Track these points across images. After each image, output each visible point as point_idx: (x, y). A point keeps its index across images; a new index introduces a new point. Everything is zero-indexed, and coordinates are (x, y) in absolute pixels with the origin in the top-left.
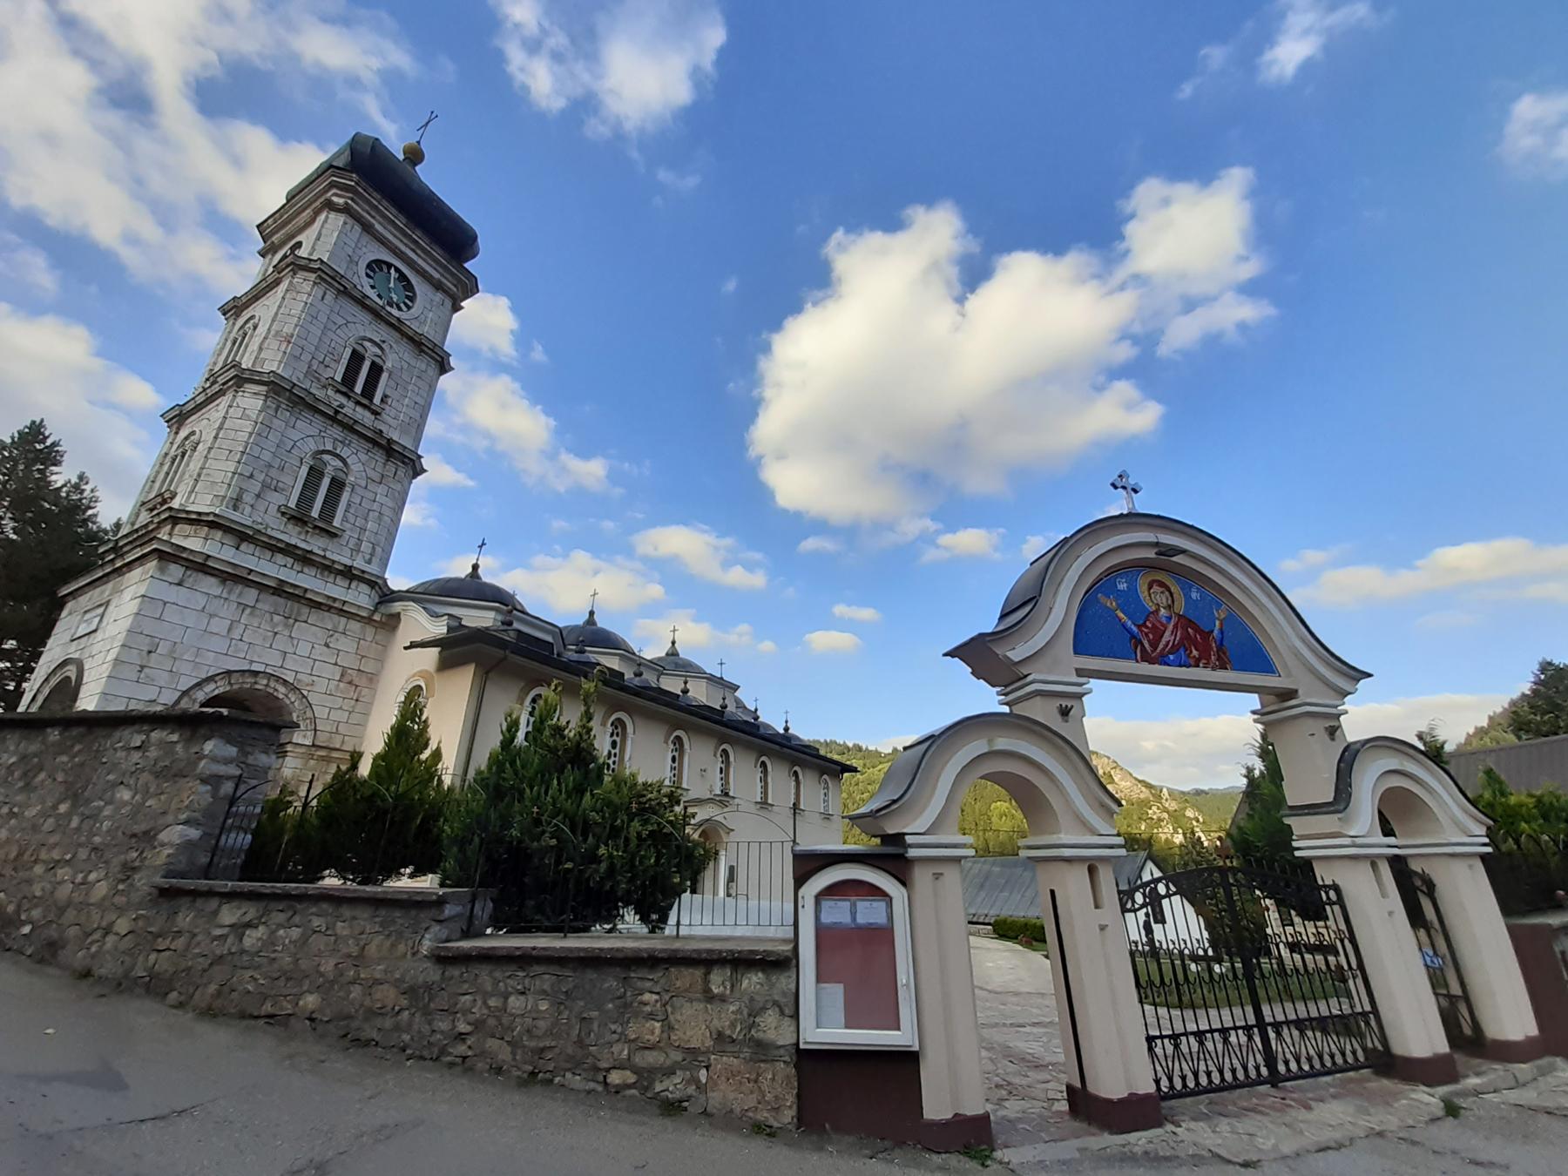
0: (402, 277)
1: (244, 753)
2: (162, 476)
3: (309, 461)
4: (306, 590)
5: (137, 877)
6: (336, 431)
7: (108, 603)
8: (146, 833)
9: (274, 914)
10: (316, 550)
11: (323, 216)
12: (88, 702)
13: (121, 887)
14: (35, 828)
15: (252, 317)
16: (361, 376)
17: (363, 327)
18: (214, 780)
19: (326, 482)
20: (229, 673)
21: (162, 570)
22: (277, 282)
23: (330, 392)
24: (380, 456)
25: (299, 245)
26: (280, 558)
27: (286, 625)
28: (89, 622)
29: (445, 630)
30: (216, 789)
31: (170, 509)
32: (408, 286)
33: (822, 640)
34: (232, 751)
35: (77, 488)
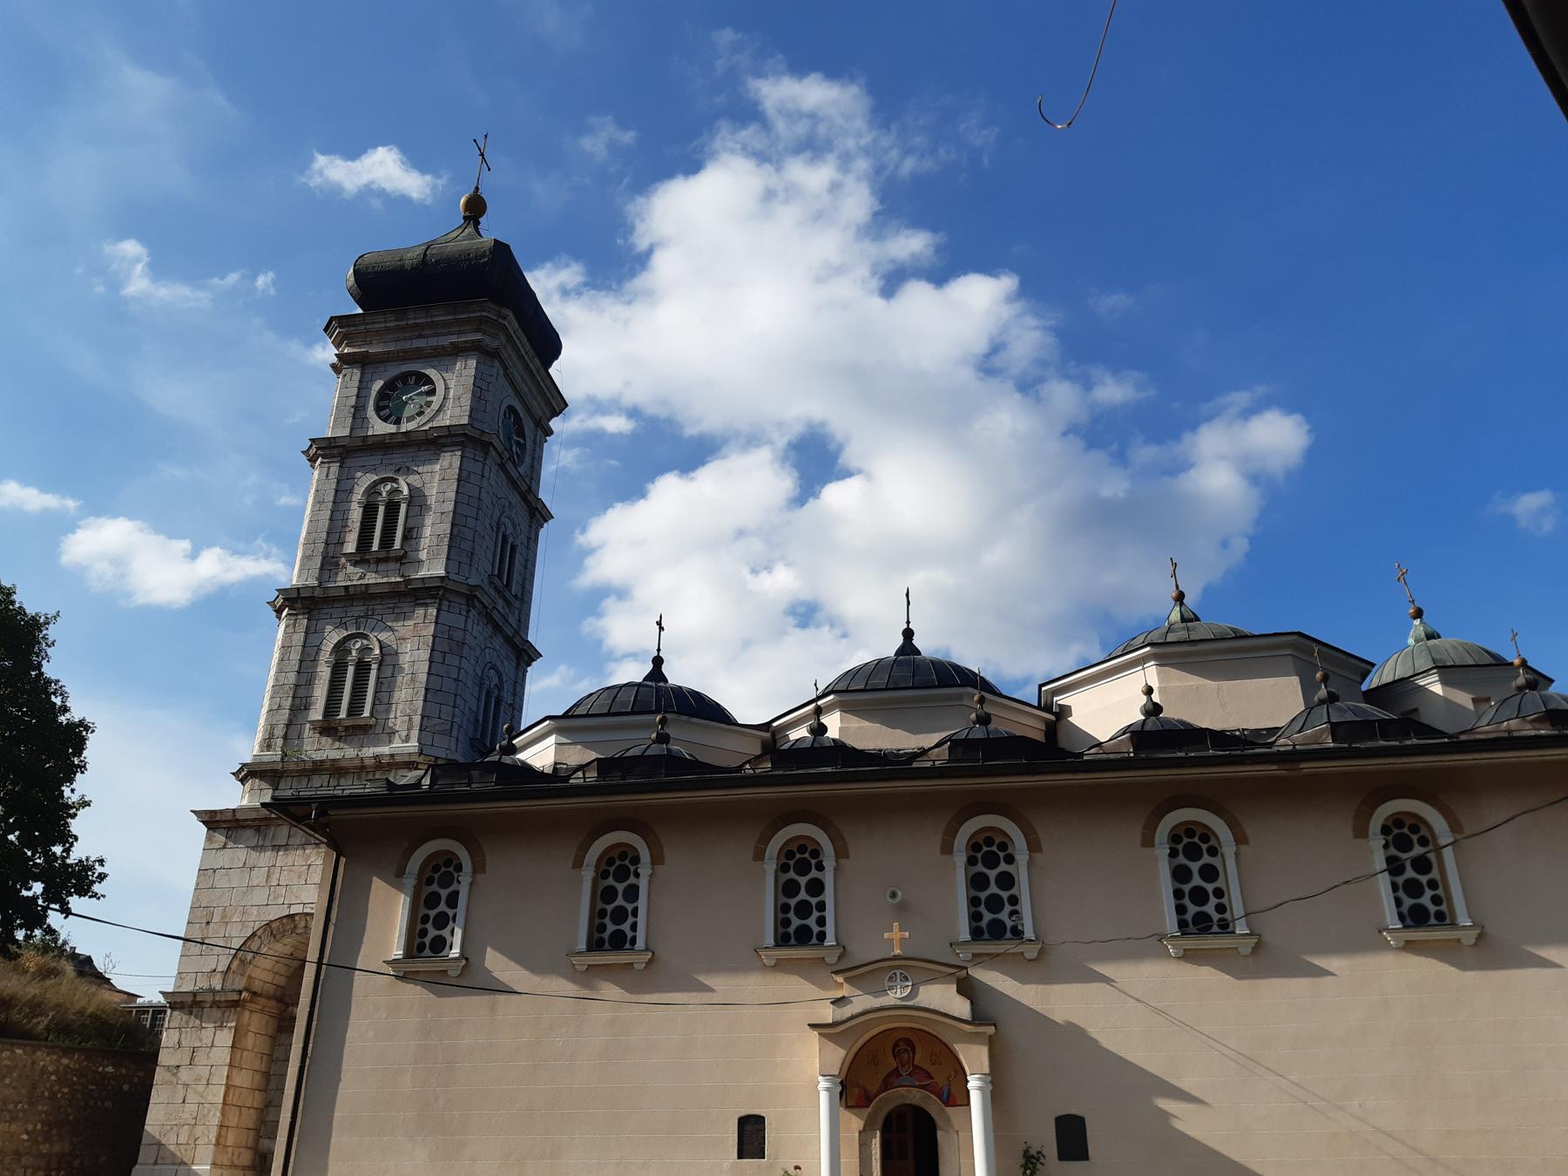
6: (358, 610)
19: (351, 670)
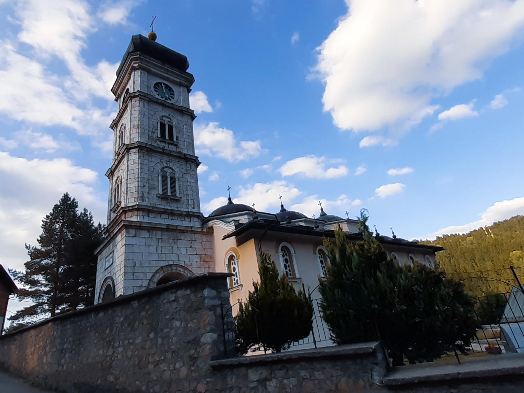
0: (167, 86)
1: (219, 293)
2: (113, 197)
3: (160, 173)
4: (177, 226)
5: (199, 362)
6: (166, 158)
7: (113, 252)
8: (194, 340)
9: (277, 372)
10: (175, 209)
11: (133, 74)
12: (119, 292)
13: (193, 368)
14: (143, 348)
15: (122, 125)
16: (167, 132)
17: (161, 112)
18: (212, 308)
19: (169, 179)
20: (162, 268)
21: (127, 232)
22: (126, 107)
23: (158, 143)
24: (184, 163)
25: (128, 89)
26: (164, 216)
27: (175, 243)
28: (109, 261)
29: (234, 228)
30: (215, 312)
31: (122, 208)
32: (170, 89)
33: (384, 190)
34: (214, 293)
35: (85, 214)
